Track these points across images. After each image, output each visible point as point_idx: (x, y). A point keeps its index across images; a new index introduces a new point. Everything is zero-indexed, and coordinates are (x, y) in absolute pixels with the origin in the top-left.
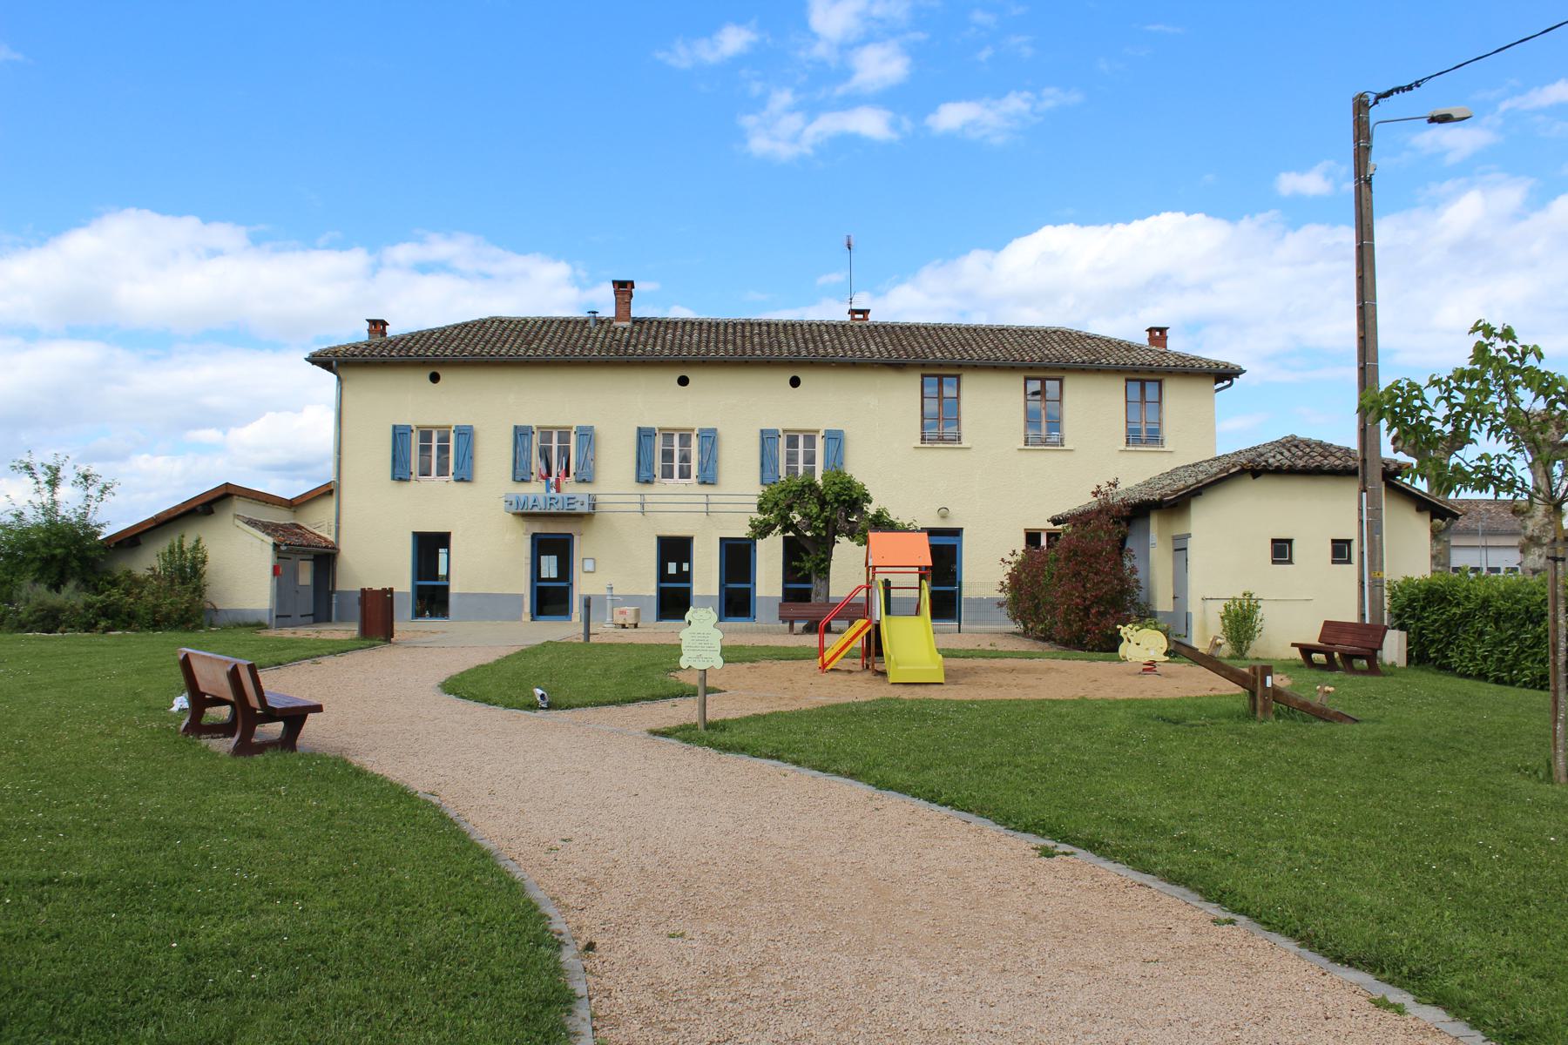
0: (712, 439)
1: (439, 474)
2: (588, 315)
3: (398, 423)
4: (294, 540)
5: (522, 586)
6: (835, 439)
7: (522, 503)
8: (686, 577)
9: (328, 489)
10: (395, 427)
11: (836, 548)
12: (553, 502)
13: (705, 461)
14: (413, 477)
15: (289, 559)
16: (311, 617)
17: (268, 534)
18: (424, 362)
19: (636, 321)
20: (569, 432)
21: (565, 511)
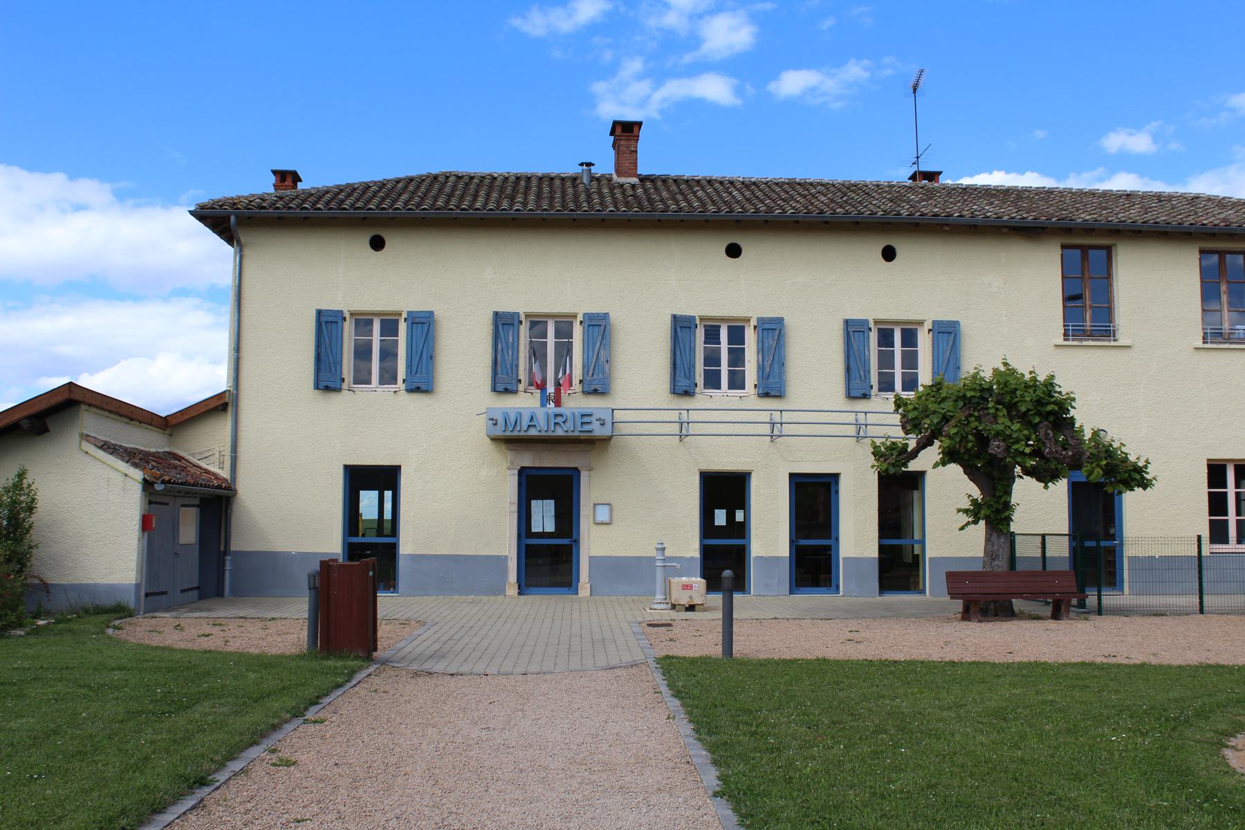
0: (777, 332)
1: (382, 381)
2: (579, 170)
3: (324, 307)
4: (172, 475)
5: (506, 545)
6: (947, 333)
7: (513, 422)
8: (740, 530)
9: (221, 402)
10: (319, 313)
11: (1015, 487)
12: (559, 420)
13: (767, 364)
14: (345, 386)
15: (167, 504)
16: (196, 592)
17: (136, 465)
18: (364, 219)
19: (643, 179)
20: (571, 324)
21: (576, 434)
